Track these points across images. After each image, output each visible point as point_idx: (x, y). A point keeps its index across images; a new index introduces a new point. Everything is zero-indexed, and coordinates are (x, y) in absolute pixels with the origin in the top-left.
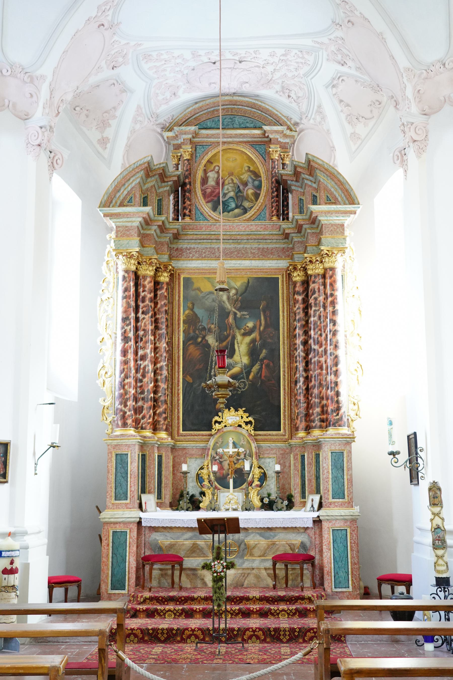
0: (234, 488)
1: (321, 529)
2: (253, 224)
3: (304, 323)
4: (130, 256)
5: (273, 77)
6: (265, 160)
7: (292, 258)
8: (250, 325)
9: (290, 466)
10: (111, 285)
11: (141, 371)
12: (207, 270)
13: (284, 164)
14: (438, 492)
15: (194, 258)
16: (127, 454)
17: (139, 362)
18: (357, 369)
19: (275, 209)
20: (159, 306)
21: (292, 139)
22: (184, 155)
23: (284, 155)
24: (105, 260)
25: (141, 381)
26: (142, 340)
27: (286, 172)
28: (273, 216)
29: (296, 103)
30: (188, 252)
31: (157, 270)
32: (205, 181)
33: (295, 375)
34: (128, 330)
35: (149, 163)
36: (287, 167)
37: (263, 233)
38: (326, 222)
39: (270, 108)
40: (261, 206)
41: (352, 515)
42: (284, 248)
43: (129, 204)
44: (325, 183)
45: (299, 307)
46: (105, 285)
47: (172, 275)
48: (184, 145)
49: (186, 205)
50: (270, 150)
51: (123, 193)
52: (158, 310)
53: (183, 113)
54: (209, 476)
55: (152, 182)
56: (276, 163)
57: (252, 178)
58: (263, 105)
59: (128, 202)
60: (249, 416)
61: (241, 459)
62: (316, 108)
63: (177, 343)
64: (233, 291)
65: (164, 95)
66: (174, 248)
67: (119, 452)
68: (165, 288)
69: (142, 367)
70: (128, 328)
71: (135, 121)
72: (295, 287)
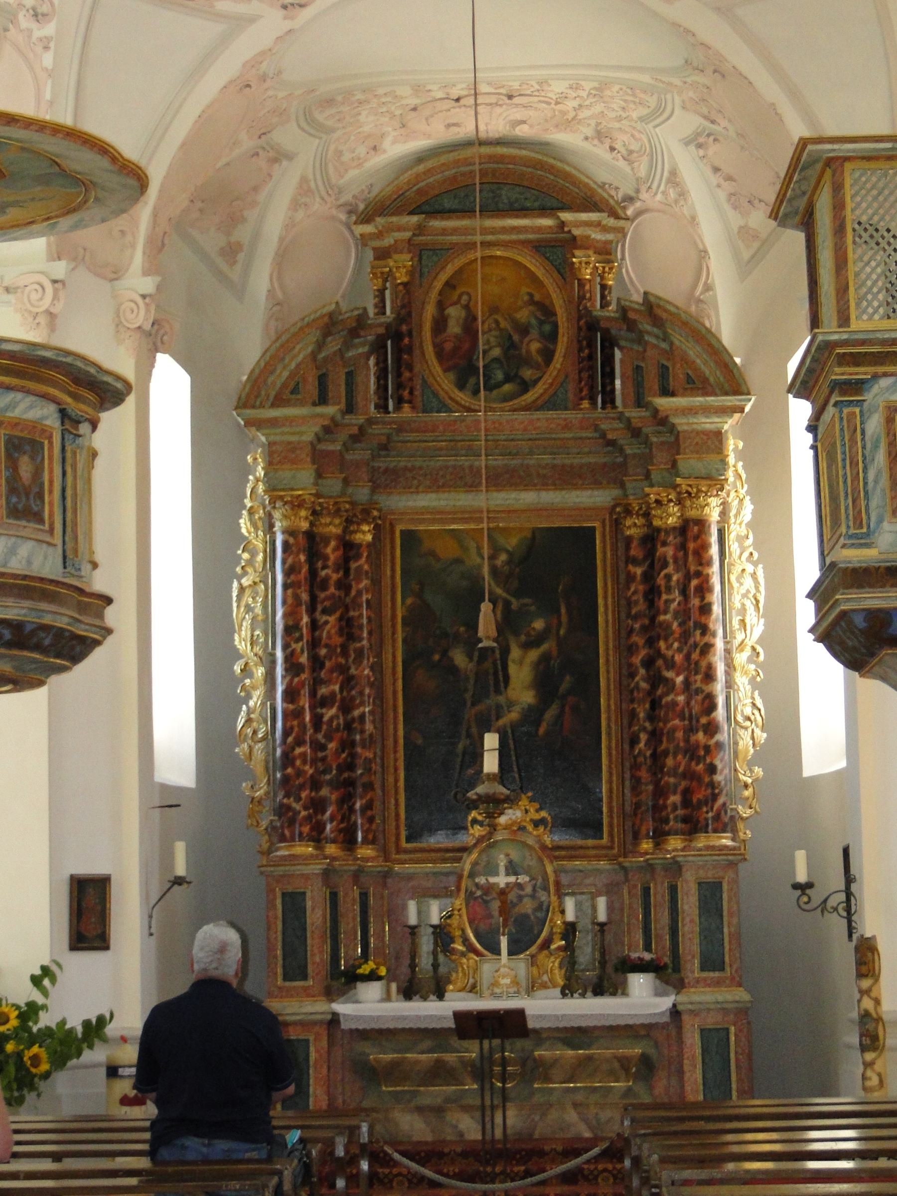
0: (511, 953)
1: (680, 1028)
2: (541, 416)
3: (647, 622)
4: (297, 504)
5: (576, 115)
6: (565, 279)
7: (622, 485)
8: (539, 625)
9: (622, 910)
10: (260, 557)
11: (325, 727)
12: (449, 513)
13: (604, 287)
14: (870, 954)
15: (421, 489)
16: (304, 893)
17: (319, 710)
18: (752, 718)
19: (586, 385)
20: (353, 593)
21: (620, 235)
22: (398, 275)
23: (604, 268)
24: (244, 507)
25: (323, 748)
26: (322, 665)
27: (607, 314)
28: (582, 399)
29: (627, 163)
30: (409, 475)
31: (349, 521)
32: (440, 324)
33: (630, 727)
34: (299, 650)
35: (331, 315)
36: (610, 293)
37: (562, 436)
38: (685, 428)
39: (574, 172)
40: (557, 376)
41: (737, 1002)
42: (605, 464)
43: (293, 396)
44: (684, 347)
45: (638, 588)
46: (246, 556)
47: (377, 528)
48: (396, 252)
49: (403, 378)
50: (574, 260)
51: (282, 375)
52: (354, 600)
53: (393, 182)
54: (463, 930)
55: (333, 345)
56: (587, 287)
57: (537, 318)
58: (559, 164)
59: (292, 393)
60: (541, 809)
61: (527, 896)
62: (666, 174)
63: (390, 664)
64: (503, 557)
65: (354, 152)
66: (380, 467)
67: (290, 889)
68: (365, 554)
69: (325, 719)
70: (298, 646)
71: (295, 205)
72: (628, 547)
